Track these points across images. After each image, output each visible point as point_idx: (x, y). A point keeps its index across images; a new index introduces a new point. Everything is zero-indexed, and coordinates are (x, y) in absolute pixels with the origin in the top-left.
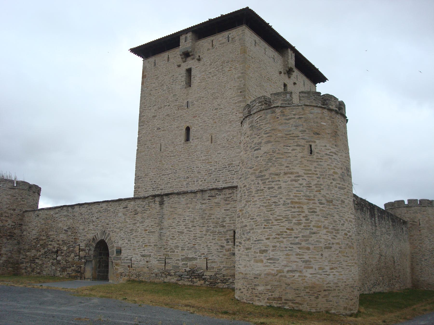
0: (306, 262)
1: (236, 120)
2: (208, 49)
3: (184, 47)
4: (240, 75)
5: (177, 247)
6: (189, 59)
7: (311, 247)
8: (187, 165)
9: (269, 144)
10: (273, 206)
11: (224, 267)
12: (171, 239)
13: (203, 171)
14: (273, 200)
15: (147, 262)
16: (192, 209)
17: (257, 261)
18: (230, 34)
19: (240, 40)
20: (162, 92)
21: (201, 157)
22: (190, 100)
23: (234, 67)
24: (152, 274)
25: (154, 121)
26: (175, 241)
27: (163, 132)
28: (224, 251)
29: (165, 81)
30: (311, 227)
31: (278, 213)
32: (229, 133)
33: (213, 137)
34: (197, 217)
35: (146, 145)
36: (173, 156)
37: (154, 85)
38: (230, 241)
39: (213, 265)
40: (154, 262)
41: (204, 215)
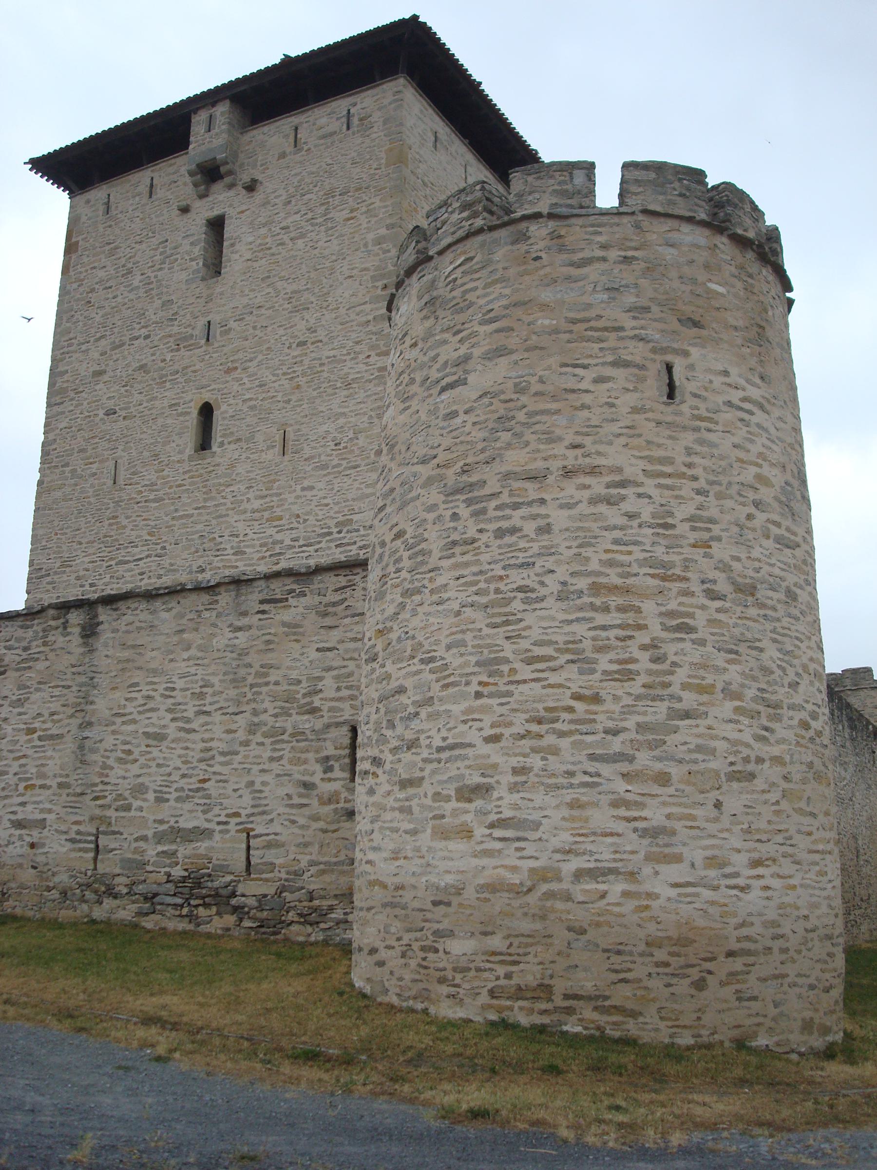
0: (652, 833)
1: (367, 376)
2: (283, 155)
3: (203, 148)
4: (383, 231)
5: (140, 790)
6: (218, 187)
7: (675, 771)
8: (200, 527)
9: (503, 361)
10: (517, 605)
11: (312, 863)
12: (120, 760)
13: (253, 546)
14: (518, 578)
15: (32, 846)
16: (200, 648)
17: (443, 834)
18: (355, 105)
19: (385, 122)
20: (126, 294)
21: (248, 500)
22: (215, 318)
23: (364, 209)
24: (49, 889)
25: (97, 387)
26: (135, 769)
27: (127, 422)
28: (315, 802)
29: (137, 258)
30: (675, 689)
31: (535, 634)
32: (341, 421)
33: (290, 436)
34: (215, 680)
35: (67, 465)
36: (155, 501)
37: (101, 274)
38: (337, 766)
39: (271, 856)
40: (57, 847)
41: (242, 672)
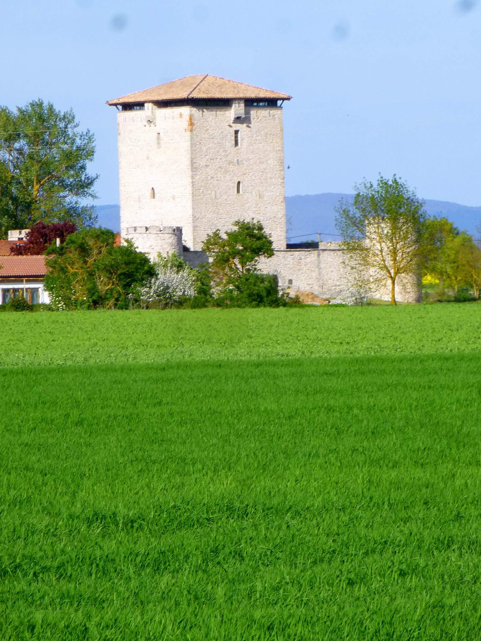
22: (240, 160)
32: (272, 193)
